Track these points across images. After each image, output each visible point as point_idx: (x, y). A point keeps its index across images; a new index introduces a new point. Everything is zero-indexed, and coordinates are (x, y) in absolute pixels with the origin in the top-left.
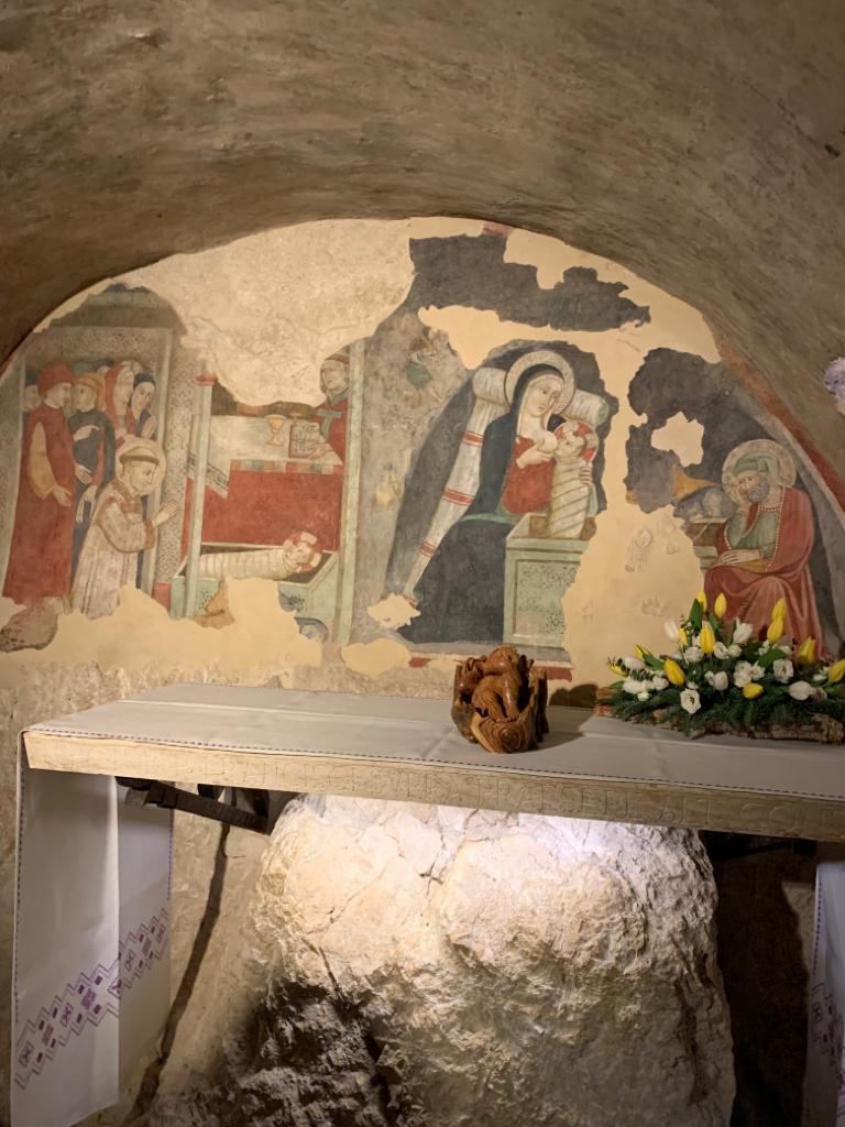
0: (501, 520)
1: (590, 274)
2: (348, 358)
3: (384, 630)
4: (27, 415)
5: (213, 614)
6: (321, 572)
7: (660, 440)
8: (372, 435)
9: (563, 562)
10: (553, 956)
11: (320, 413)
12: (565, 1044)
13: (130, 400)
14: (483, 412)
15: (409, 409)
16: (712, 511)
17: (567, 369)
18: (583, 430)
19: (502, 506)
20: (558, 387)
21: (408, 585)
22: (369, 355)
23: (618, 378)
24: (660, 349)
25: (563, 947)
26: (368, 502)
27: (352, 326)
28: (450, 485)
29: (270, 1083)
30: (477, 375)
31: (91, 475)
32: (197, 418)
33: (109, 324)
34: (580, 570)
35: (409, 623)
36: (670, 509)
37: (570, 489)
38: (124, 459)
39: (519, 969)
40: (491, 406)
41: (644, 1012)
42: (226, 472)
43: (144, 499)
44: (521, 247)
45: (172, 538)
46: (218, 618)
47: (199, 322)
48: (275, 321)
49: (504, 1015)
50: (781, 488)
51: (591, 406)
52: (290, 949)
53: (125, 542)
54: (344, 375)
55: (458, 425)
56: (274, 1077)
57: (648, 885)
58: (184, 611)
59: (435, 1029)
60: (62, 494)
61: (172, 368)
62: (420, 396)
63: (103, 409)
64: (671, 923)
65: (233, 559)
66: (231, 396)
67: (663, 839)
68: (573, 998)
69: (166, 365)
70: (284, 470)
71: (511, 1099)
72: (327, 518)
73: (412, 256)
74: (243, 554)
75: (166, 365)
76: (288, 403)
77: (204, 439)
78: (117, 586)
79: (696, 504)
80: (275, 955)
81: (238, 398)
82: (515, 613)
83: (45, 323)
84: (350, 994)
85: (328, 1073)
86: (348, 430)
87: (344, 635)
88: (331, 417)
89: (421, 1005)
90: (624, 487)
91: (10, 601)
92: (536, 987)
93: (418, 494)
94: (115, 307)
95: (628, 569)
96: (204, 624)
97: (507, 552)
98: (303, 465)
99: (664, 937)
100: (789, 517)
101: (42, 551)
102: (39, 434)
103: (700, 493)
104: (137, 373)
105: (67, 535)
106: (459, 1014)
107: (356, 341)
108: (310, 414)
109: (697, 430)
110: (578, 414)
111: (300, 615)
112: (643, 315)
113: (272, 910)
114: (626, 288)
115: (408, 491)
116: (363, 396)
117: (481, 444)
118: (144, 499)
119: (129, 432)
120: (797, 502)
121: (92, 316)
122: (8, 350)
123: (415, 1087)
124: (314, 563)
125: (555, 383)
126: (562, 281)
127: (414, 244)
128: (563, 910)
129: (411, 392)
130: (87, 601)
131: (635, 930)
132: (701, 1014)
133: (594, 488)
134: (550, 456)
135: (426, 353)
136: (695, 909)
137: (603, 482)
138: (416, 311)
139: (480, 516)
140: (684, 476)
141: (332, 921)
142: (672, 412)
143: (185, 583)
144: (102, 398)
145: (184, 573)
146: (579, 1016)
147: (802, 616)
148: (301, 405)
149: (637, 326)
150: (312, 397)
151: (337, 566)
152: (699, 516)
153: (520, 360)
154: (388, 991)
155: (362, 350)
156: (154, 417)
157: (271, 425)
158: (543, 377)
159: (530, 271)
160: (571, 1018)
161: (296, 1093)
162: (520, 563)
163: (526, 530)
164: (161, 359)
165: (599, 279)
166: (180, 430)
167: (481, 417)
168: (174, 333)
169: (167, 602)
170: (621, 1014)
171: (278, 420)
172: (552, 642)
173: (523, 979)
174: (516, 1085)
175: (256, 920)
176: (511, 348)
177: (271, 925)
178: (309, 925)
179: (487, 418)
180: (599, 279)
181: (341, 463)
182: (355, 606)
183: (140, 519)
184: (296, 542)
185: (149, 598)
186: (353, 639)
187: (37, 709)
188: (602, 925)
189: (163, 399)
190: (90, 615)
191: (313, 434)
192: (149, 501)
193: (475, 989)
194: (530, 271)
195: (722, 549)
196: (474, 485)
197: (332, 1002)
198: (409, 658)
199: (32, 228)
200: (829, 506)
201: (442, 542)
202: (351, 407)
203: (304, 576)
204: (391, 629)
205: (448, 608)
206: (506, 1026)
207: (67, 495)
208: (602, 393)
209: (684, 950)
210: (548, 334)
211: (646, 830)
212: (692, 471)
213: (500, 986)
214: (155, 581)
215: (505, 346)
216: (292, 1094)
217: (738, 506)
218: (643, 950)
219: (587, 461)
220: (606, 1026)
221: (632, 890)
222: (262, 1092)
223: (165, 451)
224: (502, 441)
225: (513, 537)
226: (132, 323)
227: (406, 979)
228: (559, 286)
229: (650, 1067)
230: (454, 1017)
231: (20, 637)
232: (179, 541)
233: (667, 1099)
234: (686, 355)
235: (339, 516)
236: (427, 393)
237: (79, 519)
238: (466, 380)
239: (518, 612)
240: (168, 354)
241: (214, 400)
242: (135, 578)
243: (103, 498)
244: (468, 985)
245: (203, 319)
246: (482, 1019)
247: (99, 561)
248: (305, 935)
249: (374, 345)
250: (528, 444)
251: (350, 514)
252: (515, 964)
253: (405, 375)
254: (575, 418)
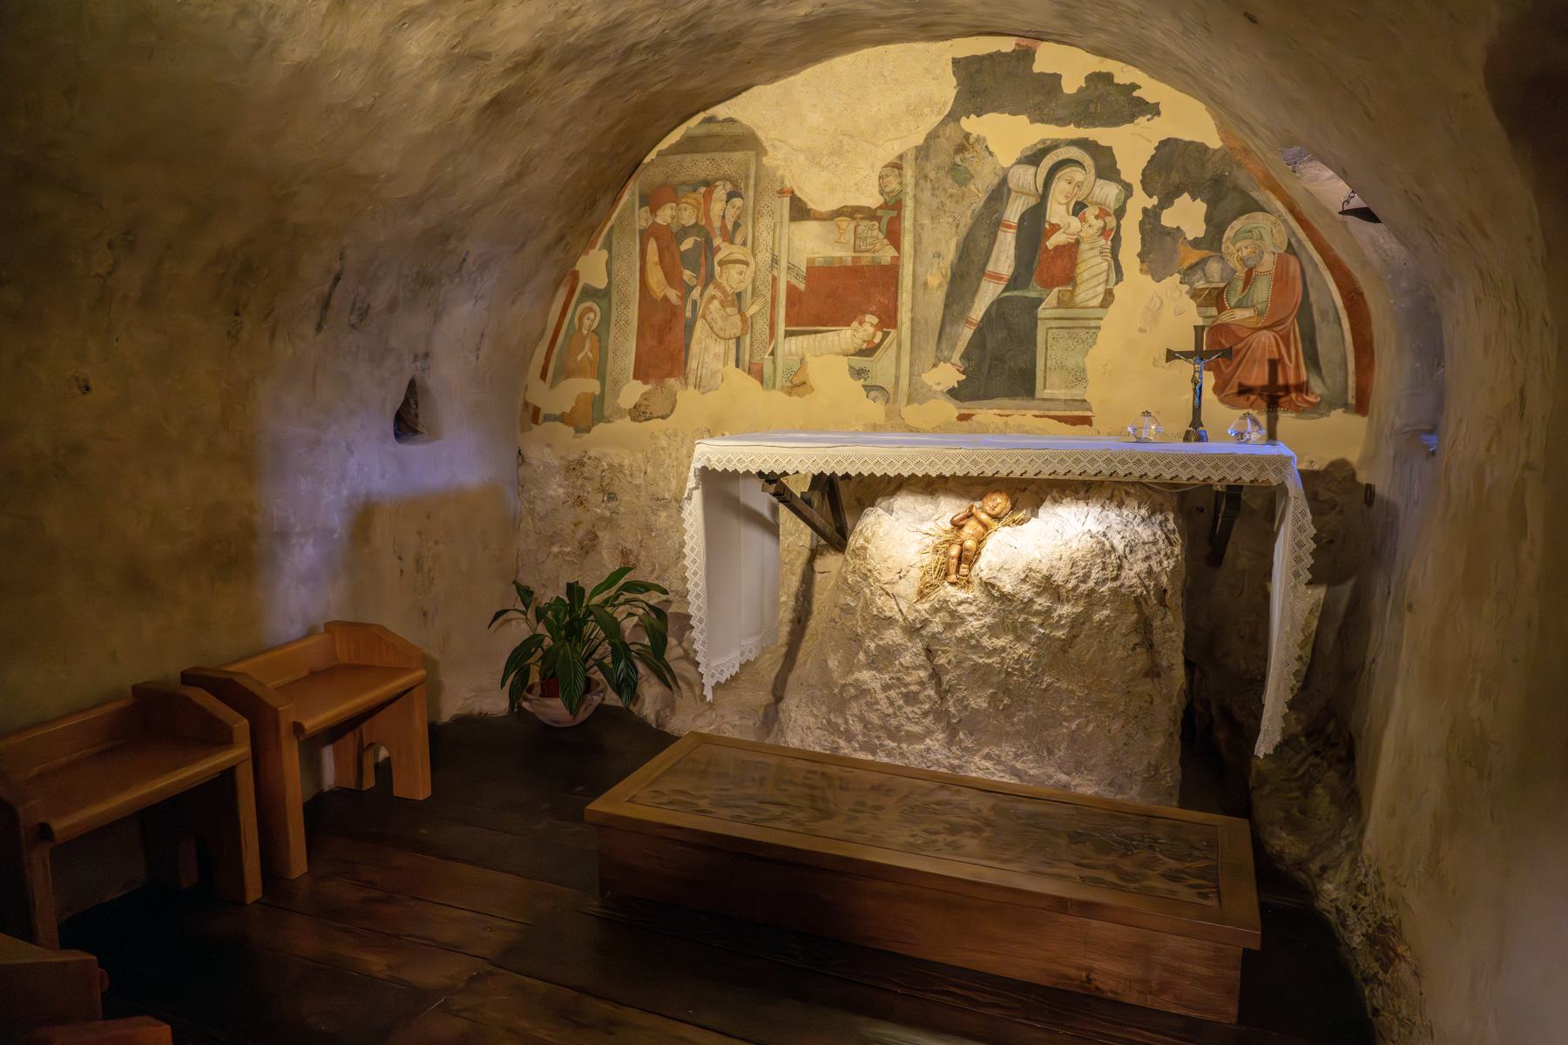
0: (1032, 294)
1: (1108, 77)
2: (902, 165)
3: (936, 392)
4: (642, 232)
5: (797, 386)
6: (883, 346)
7: (1168, 219)
8: (923, 229)
9: (1086, 328)
10: (1051, 584)
11: (879, 213)
12: (1059, 639)
13: (724, 213)
14: (1017, 203)
15: (954, 204)
16: (1213, 277)
17: (1088, 161)
18: (1103, 214)
19: (1034, 283)
21: (955, 354)
22: (919, 160)
23: (1132, 166)
24: (1169, 139)
25: (1059, 578)
26: (920, 285)
27: (904, 137)
28: (990, 268)
29: (862, 679)
30: (1011, 171)
31: (696, 278)
32: (778, 225)
33: (703, 151)
34: (1101, 334)
35: (956, 386)
36: (1177, 277)
37: (1092, 266)
38: (721, 263)
39: (1029, 594)
40: (1024, 197)
41: (1112, 615)
42: (804, 268)
43: (739, 295)
44: (1048, 58)
45: (762, 326)
46: (801, 390)
47: (777, 143)
48: (840, 138)
49: (1019, 625)
50: (1274, 253)
51: (1108, 192)
52: (872, 594)
53: (725, 330)
54: (899, 179)
55: (995, 216)
56: (865, 675)
57: (1126, 546)
58: (774, 385)
59: (972, 636)
60: (673, 295)
61: (756, 186)
62: (963, 192)
63: (703, 222)
64: (1141, 567)
65: (811, 341)
66: (805, 204)
67: (1143, 520)
68: (1065, 609)
69: (752, 182)
70: (850, 264)
71: (1022, 676)
72: (886, 302)
73: (954, 73)
74: (819, 335)
75: (752, 182)
76: (852, 207)
77: (785, 242)
78: (721, 367)
79: (1199, 272)
80: (862, 600)
81: (811, 205)
82: (1045, 372)
83: (652, 155)
84: (913, 620)
85: (900, 671)
86: (902, 225)
87: (903, 398)
88: (888, 218)
89: (962, 623)
90: (1138, 260)
91: (639, 382)
92: (1040, 605)
93: (962, 277)
94: (708, 136)
95: (1142, 330)
96: (790, 394)
97: (1039, 322)
98: (866, 258)
99: (1132, 574)
100: (1281, 279)
101: (661, 342)
102: (652, 247)
103: (1201, 264)
104: (728, 191)
105: (679, 329)
106: (988, 627)
107: (909, 150)
108: (870, 214)
109: (1200, 207)
110: (1099, 200)
111: (867, 383)
112: (1154, 110)
113: (859, 569)
114: (1140, 87)
115: (954, 274)
116: (915, 196)
117: (1015, 231)
118: (739, 295)
119: (724, 241)
120: (1288, 266)
121: (690, 145)
122: (626, 179)
123: (958, 675)
124: (877, 340)
125: (1078, 174)
126: (1084, 85)
127: (956, 62)
128: (1061, 558)
129: (954, 190)
130: (698, 379)
131: (1112, 569)
132: (1156, 623)
133: (1112, 263)
134: (1075, 237)
135: (968, 156)
136: (1161, 562)
137: (1120, 257)
138: (958, 120)
139: (1016, 293)
140: (1190, 248)
141: (900, 578)
142: (1178, 193)
143: (774, 362)
144: (701, 212)
145: (772, 354)
146: (1068, 620)
147: (1291, 362)
148: (863, 207)
149: (1148, 120)
150: (872, 200)
151: (895, 345)
152: (1202, 282)
153: (1048, 156)
154: (940, 617)
155: (913, 157)
156: (743, 227)
157: (839, 227)
158: (1068, 170)
159: (1057, 77)
160: (1063, 622)
161: (879, 685)
162: (1050, 331)
163: (1055, 302)
164: (747, 177)
165: (1116, 80)
166: (765, 237)
167: (1015, 206)
168: (757, 155)
169: (760, 378)
170: (1097, 617)
171: (844, 222)
172: (1076, 395)
173: (1031, 601)
174: (1027, 667)
175: (848, 577)
176: (1039, 146)
177: (858, 579)
178: (885, 578)
179: (1020, 208)
180: (1116, 80)
181: (896, 254)
182: (911, 374)
183: (736, 312)
184: (861, 324)
185: (746, 375)
186: (910, 401)
187: (666, 465)
188: (1087, 565)
189: (750, 211)
190: (701, 390)
191: (874, 231)
192: (743, 294)
193: (999, 610)
194: (1057, 77)
195: (1221, 308)
196: (1009, 267)
197: (902, 627)
198: (957, 415)
199: (659, 87)
200: (1316, 265)
201: (984, 315)
202: (905, 206)
203: (869, 351)
204: (942, 391)
205: (989, 371)
206: (1020, 632)
207: (677, 295)
208: (1119, 181)
209: (1147, 583)
210: (1071, 132)
211: (1131, 515)
212: (1196, 243)
213: (1016, 606)
214: (750, 363)
215: (1035, 145)
216: (877, 686)
217: (1236, 272)
218: (1115, 579)
219: (1107, 240)
220: (1087, 626)
221: (1112, 547)
222: (857, 684)
223: (755, 256)
224: (1034, 225)
225: (1044, 309)
226: (722, 148)
227: (952, 607)
228: (1081, 90)
229: (1116, 650)
230: (985, 629)
231: (648, 411)
232: (768, 328)
233: (1128, 671)
234: (1191, 143)
235: (897, 300)
236: (969, 190)
237: (688, 314)
238: (1002, 177)
239: (1048, 372)
240: (753, 172)
241: (791, 208)
242: (734, 359)
243: (706, 296)
244: (994, 609)
245: (780, 141)
246: (1004, 630)
247: (706, 348)
248: (881, 585)
249: (923, 152)
250: (1055, 228)
251: (905, 299)
252: (1027, 591)
253: (949, 176)
254: (1096, 204)
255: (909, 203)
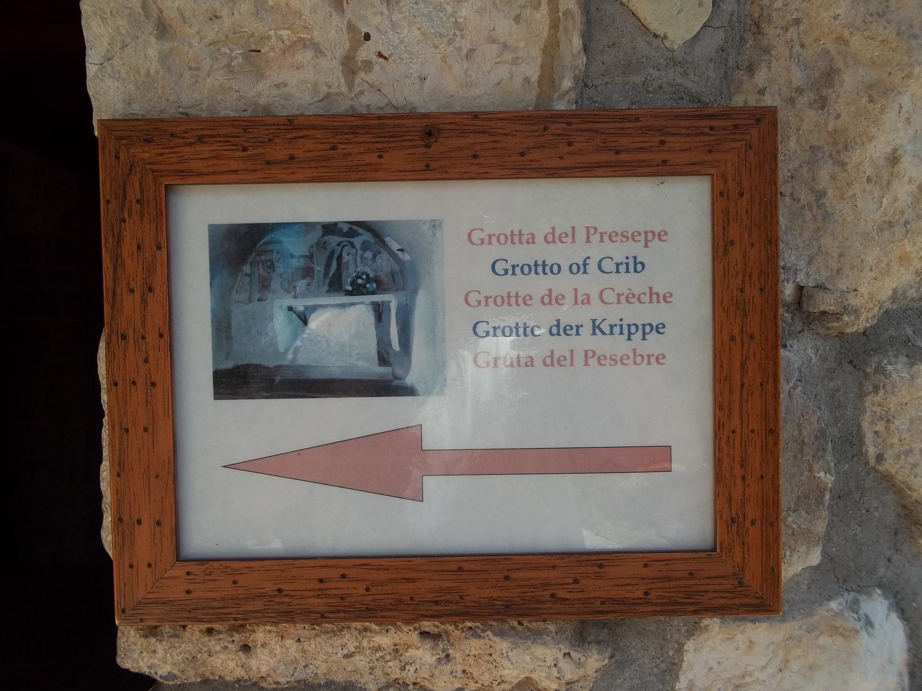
17: (349, 244)
20: (348, 249)
23: (358, 245)
43: (281, 274)
51: (353, 251)
88: (310, 257)
102: (260, 265)
108: (307, 257)
118: (281, 274)
224: (340, 258)
249: (318, 244)
255: (315, 254)
